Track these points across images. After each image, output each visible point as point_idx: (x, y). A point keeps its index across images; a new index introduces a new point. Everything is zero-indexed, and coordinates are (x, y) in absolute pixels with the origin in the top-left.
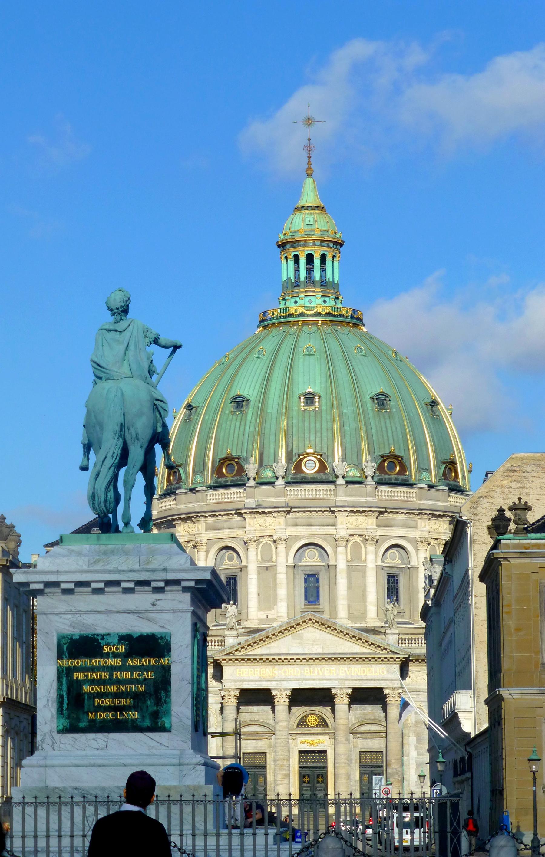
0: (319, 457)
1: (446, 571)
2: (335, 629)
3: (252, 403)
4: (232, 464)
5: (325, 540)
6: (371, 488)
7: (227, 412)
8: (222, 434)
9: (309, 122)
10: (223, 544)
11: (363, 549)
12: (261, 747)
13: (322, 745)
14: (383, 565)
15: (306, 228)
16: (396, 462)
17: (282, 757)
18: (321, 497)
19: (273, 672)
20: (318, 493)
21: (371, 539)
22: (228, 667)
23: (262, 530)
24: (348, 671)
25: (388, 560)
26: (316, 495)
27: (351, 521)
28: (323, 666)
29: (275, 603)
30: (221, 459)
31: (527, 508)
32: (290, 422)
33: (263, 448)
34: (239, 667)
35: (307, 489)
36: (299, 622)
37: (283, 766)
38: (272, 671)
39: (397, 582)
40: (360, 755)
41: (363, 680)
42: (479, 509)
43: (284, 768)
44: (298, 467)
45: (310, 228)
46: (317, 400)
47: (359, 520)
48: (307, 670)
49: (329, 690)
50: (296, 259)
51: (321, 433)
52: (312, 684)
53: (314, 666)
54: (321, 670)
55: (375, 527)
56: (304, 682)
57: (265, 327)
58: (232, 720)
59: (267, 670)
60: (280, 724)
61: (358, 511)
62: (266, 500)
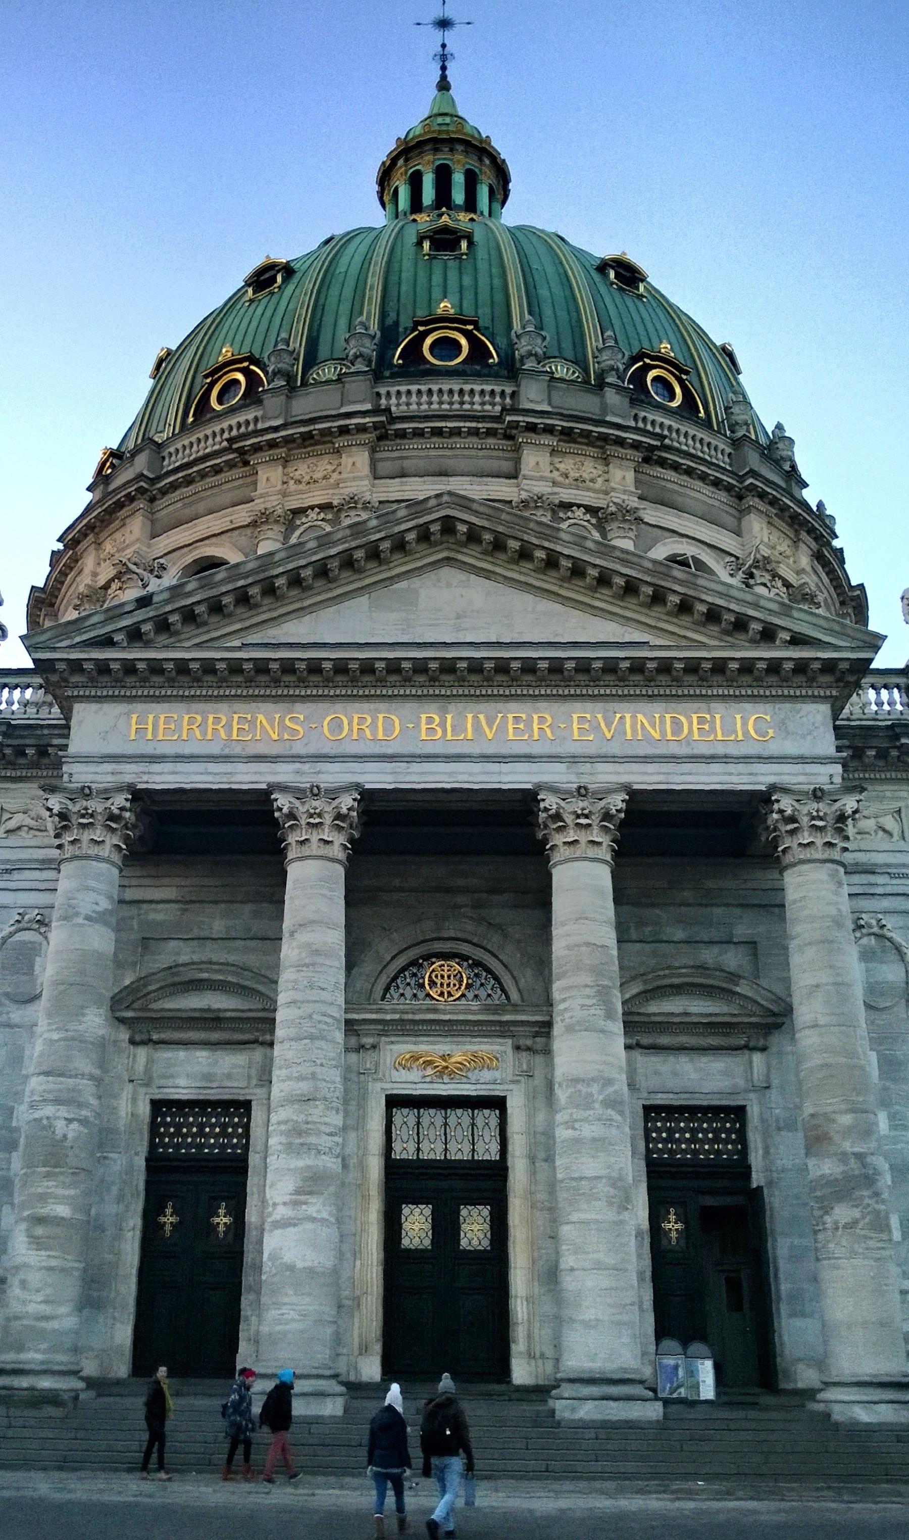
0: (470, 327)
2: (552, 562)
3: (298, 276)
4: (236, 382)
6: (618, 397)
9: (444, 24)
12: (229, 1076)
13: (487, 1075)
15: (437, 128)
17: (304, 1087)
18: (477, 407)
19: (283, 727)
20: (467, 398)
21: (624, 516)
22: (94, 707)
23: (302, 492)
24: (609, 726)
26: (462, 403)
27: (562, 467)
28: (500, 706)
32: (393, 278)
33: (319, 331)
34: (140, 706)
35: (435, 388)
36: (404, 527)
37: (307, 1132)
38: (282, 719)
40: (647, 1119)
41: (674, 759)
43: (312, 1140)
44: (413, 351)
45: (444, 128)
46: (464, 245)
47: (589, 468)
48: (430, 720)
50: (416, 181)
51: (476, 294)
52: (451, 774)
53: (461, 706)
54: (490, 722)
55: (633, 489)
56: (415, 767)
58: (88, 918)
59: (261, 717)
60: (303, 937)
61: (586, 434)
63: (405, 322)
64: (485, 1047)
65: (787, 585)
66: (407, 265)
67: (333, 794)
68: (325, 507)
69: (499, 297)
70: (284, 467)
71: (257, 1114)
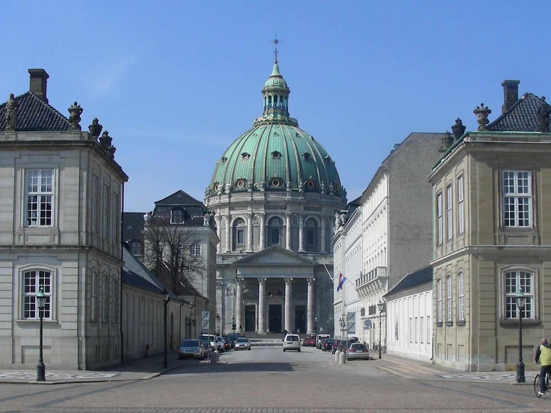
1: (359, 209)
2: (286, 253)
5: (281, 215)
7: (240, 160)
8: (238, 169)
9: (276, 42)
10: (237, 217)
11: (298, 220)
13: (280, 302)
14: (306, 226)
15: (274, 85)
16: (312, 182)
25: (309, 224)
29: (259, 242)
30: (238, 180)
31: (487, 112)
39: (312, 234)
42: (392, 163)
44: (270, 184)
45: (276, 85)
46: (279, 155)
49: (283, 278)
55: (303, 210)
57: (256, 126)
62: (256, 197)
63: (269, 176)
64: (280, 299)
65: (329, 216)
66: (270, 161)
67: (264, 279)
68: (258, 213)
69: (285, 170)
70: (252, 206)
71: (256, 307)
